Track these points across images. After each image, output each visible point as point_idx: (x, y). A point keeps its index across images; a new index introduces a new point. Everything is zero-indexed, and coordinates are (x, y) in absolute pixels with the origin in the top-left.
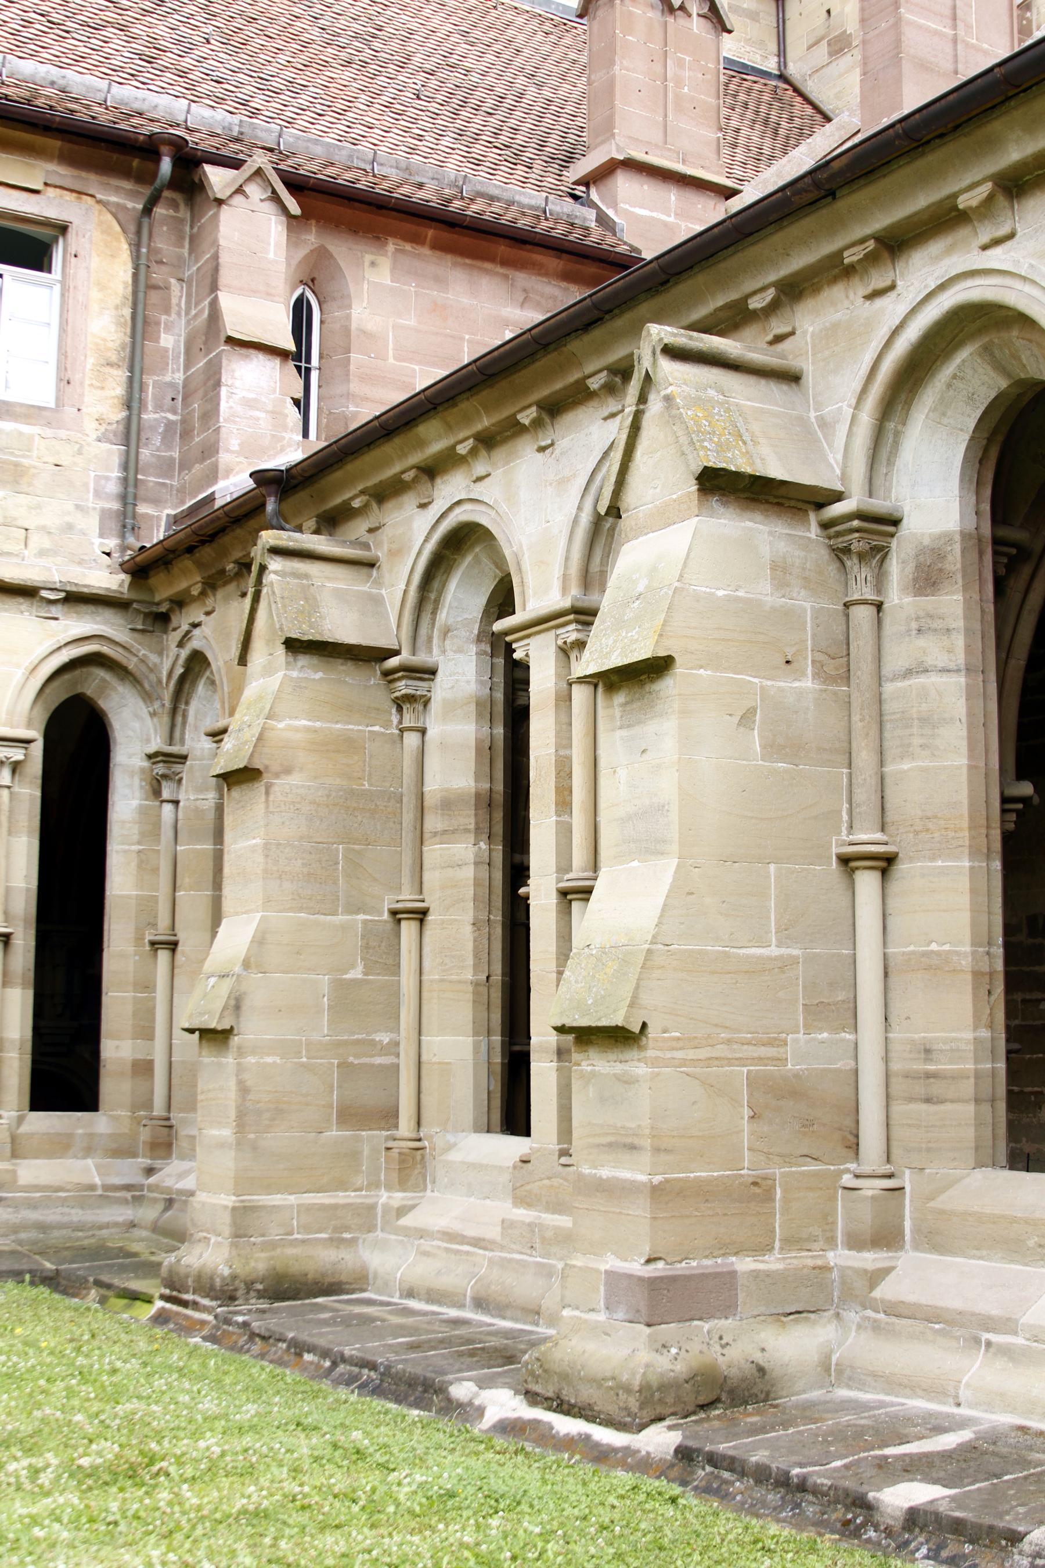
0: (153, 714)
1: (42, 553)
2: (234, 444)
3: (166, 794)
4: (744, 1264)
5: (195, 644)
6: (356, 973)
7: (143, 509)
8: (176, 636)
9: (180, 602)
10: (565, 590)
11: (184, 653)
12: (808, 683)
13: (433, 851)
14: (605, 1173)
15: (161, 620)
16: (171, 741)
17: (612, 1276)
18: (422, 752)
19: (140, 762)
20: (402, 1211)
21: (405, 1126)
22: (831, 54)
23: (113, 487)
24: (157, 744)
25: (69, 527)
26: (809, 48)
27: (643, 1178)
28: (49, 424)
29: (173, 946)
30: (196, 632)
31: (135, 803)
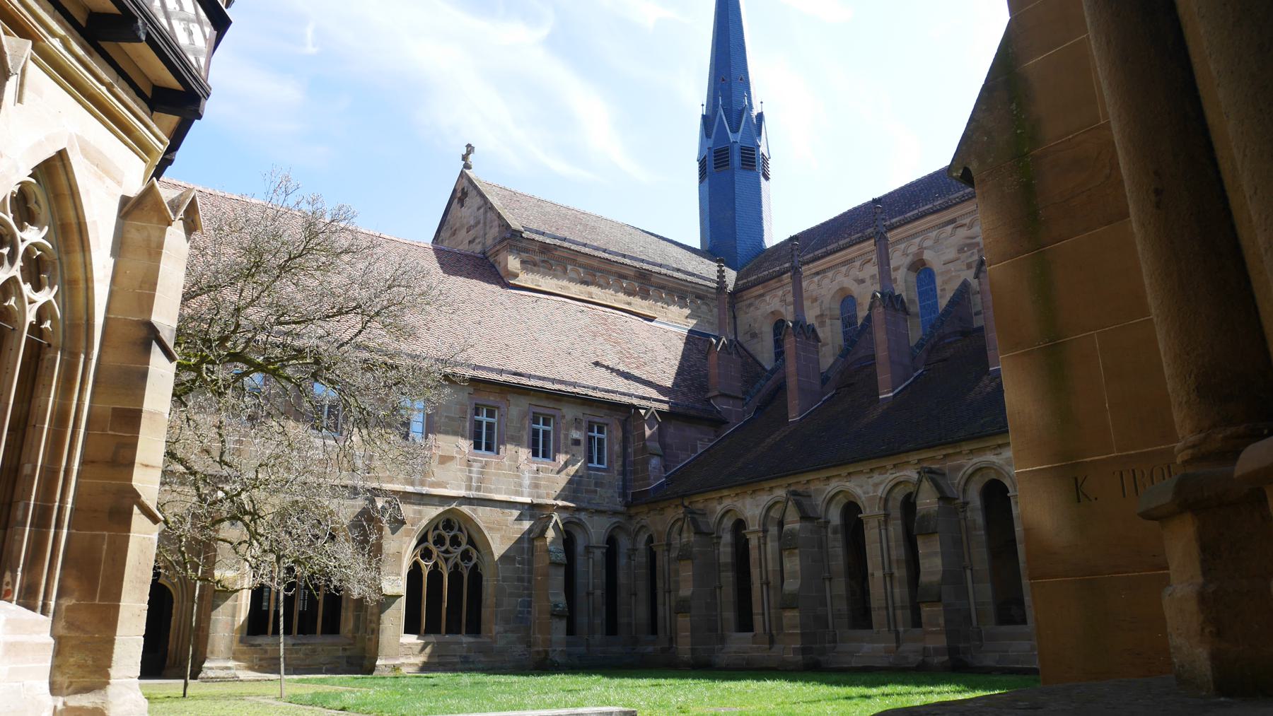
0: (629, 539)
1: (608, 503)
2: (652, 478)
3: (632, 558)
4: (814, 646)
5: (643, 522)
6: (709, 600)
7: (628, 491)
8: (636, 521)
9: (637, 514)
10: (759, 526)
11: (638, 526)
12: (816, 550)
13: (723, 574)
14: (790, 632)
15: (631, 517)
16: (634, 546)
17: (794, 648)
18: (719, 553)
19: (626, 551)
20: (722, 649)
21: (719, 632)
22: (751, 337)
23: (620, 486)
24: (630, 547)
25: (613, 496)
26: (744, 334)
27: (799, 632)
28: (607, 472)
29: (636, 595)
30: (643, 521)
31: (625, 561)
